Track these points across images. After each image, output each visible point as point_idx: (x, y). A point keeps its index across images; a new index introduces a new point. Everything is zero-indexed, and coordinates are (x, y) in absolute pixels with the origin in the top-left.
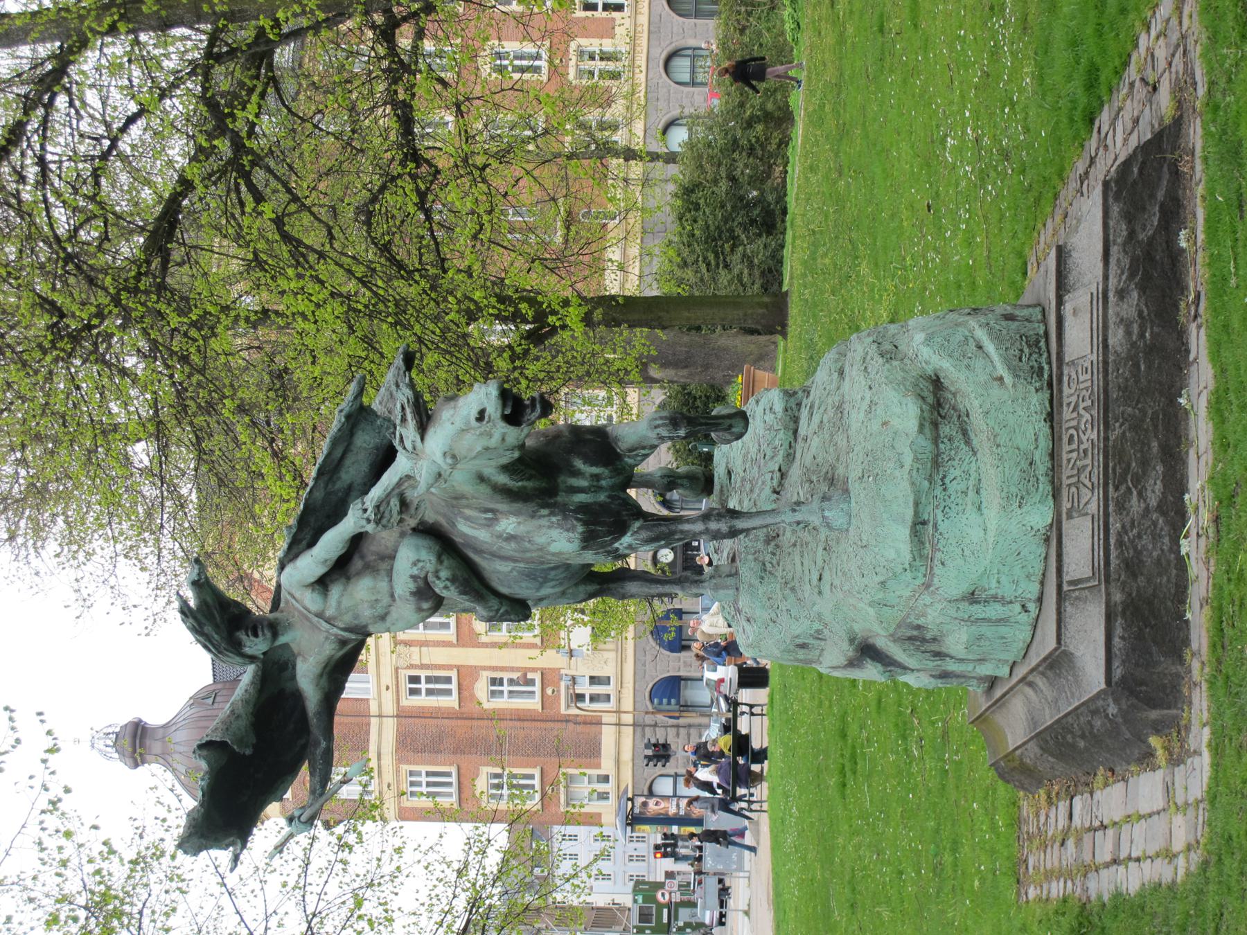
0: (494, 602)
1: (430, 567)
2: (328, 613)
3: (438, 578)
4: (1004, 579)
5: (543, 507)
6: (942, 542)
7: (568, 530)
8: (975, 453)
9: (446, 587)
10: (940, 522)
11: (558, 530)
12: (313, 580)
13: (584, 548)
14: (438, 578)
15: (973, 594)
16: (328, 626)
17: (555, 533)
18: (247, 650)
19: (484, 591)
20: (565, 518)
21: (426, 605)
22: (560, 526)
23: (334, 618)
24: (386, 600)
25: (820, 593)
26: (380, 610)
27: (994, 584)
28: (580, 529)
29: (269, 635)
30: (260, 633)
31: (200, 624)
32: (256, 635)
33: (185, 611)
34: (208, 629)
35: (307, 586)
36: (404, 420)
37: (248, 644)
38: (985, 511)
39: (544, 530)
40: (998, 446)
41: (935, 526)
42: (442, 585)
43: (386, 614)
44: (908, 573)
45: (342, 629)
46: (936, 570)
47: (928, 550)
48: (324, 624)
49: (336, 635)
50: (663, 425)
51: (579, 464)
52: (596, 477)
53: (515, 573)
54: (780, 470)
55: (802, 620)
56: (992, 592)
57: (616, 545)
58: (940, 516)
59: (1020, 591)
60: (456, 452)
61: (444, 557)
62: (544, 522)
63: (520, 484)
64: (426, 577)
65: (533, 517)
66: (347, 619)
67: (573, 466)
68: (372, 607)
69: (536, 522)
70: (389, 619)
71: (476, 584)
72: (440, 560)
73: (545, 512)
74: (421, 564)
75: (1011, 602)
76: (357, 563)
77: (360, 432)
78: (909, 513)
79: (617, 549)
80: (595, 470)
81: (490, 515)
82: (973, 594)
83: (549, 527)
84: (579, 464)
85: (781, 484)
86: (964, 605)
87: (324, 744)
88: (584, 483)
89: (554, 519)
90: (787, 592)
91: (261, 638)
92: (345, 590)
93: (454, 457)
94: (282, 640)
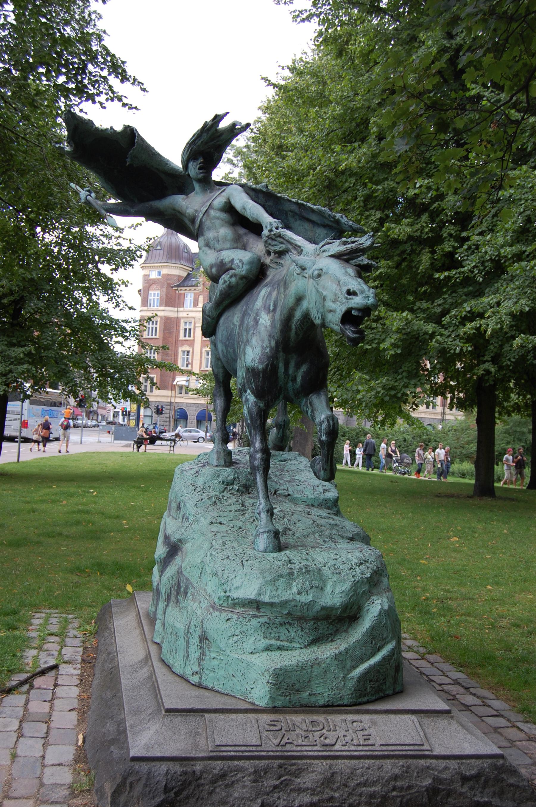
0: (215, 314)
5: (277, 343)
6: (244, 621)
7: (260, 359)
8: (306, 647)
9: (225, 282)
10: (258, 620)
11: (260, 352)
12: (233, 202)
13: (247, 369)
14: (231, 277)
15: (206, 639)
16: (204, 212)
17: (258, 350)
18: (191, 164)
19: (221, 308)
20: (269, 358)
21: (214, 270)
22: (263, 354)
23: (208, 216)
24: (218, 247)
25: (212, 523)
27: (213, 655)
28: (261, 367)
29: (200, 176)
30: (201, 171)
31: (209, 129)
32: (199, 169)
33: (218, 119)
34: (205, 136)
35: (229, 199)
36: (345, 243)
37: (195, 164)
38: (265, 654)
39: (260, 343)
40: (312, 666)
41: (255, 616)
42: (226, 279)
44: (223, 594)
46: (224, 614)
48: (205, 209)
49: (198, 216)
50: (329, 425)
51: (304, 368)
52: (294, 380)
53: (232, 326)
54: (289, 495)
55: (195, 508)
56: (207, 653)
57: (249, 391)
58: (262, 620)
59: (207, 672)
60: (322, 278)
61: (244, 280)
62: (266, 343)
63: (294, 327)
64: (231, 269)
65: (270, 336)
66: (207, 223)
67: (302, 364)
68: (214, 238)
69: (266, 338)
71: (226, 302)
73: (273, 343)
74: (241, 265)
75: (199, 665)
76: (242, 231)
77: (326, 232)
78: (266, 598)
79: (246, 392)
80: (299, 379)
81: (272, 308)
82: (206, 639)
83: (262, 347)
84: (304, 368)
85: (281, 495)
86: (198, 631)
88: (291, 371)
89: (268, 350)
90: (214, 500)
91: (198, 171)
92: (226, 222)
93: (319, 276)
94: (197, 186)
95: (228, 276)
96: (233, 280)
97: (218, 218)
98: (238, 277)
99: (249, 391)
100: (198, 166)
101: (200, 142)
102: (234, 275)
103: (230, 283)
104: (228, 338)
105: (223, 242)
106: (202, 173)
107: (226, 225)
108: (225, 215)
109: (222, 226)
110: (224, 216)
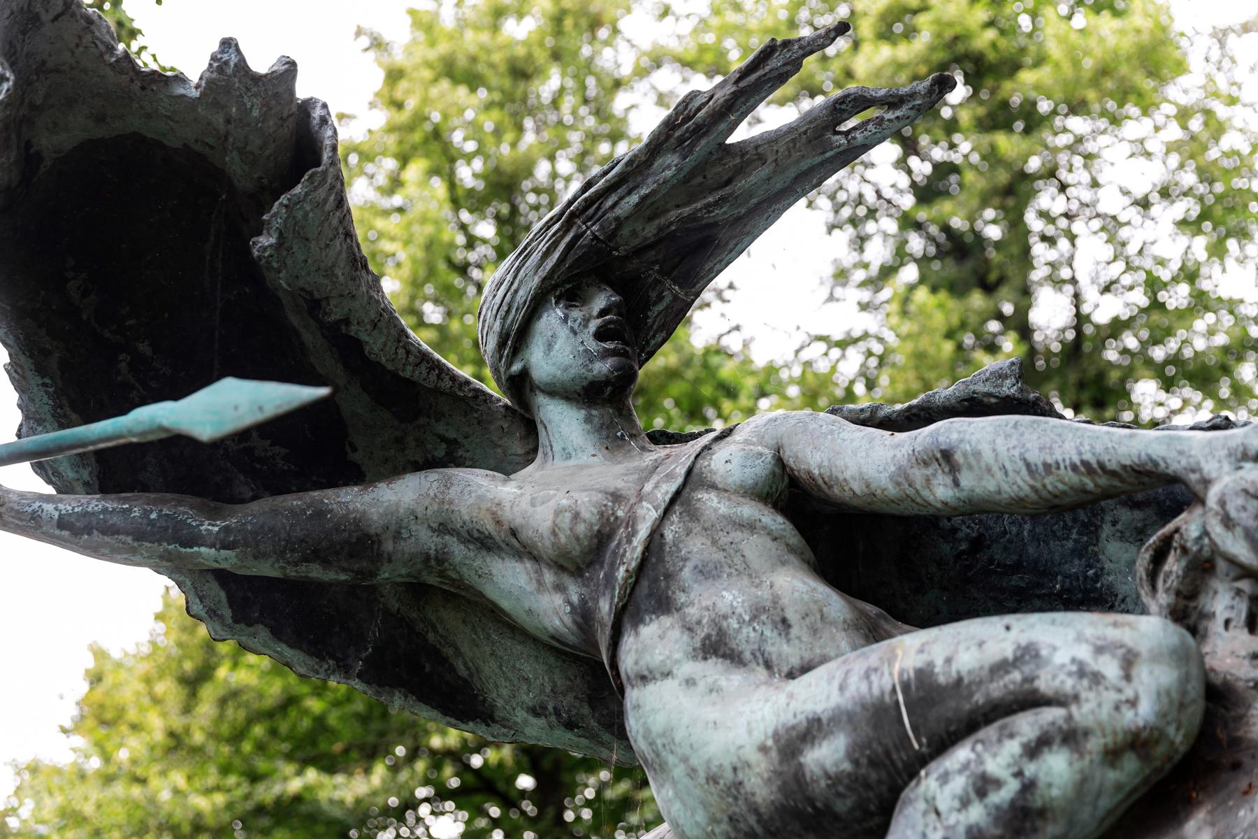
1: (1092, 709)
2: (711, 503)
3: (1034, 750)
9: (983, 785)
14: (1034, 750)
23: (693, 514)
24: (788, 652)
26: (746, 638)
29: (602, 368)
30: (609, 345)
31: (700, 131)
32: (600, 335)
34: (669, 165)
37: (576, 314)
43: (734, 658)
45: (656, 533)
49: (631, 522)
61: (1131, 764)
64: (1030, 700)
70: (712, 670)
72: (1138, 742)
74: (1110, 668)
87: (210, 527)
91: (593, 345)
92: (791, 549)
94: (564, 423)
95: (1013, 747)
96: (1057, 768)
97: (751, 527)
98: (1094, 745)
100: (594, 325)
101: (634, 199)
102: (1071, 737)
103: (1029, 786)
105: (814, 631)
106: (613, 353)
107: (792, 558)
108: (780, 519)
109: (783, 563)
110: (773, 520)
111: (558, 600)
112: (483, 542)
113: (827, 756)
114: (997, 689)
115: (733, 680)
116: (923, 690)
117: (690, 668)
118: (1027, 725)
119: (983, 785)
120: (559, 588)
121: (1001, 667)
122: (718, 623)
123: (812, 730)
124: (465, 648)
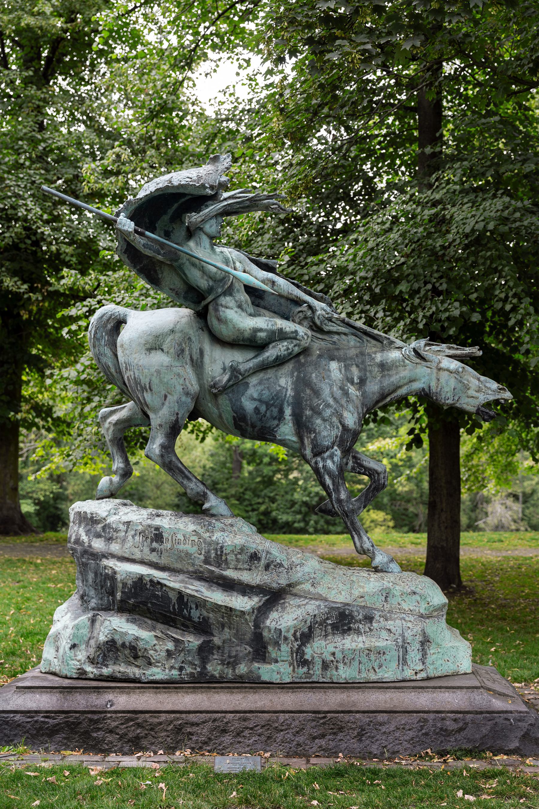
3: (295, 346)
4: (434, 656)
9: (288, 349)
14: (295, 346)
17: (356, 415)
27: (432, 652)
42: (290, 347)
43: (242, 309)
44: (426, 605)
47: (435, 614)
53: (278, 388)
62: (360, 410)
64: (295, 339)
65: (363, 404)
70: (239, 310)
74: (306, 337)
79: (333, 448)
81: (356, 380)
86: (419, 638)
99: (336, 448)
104: (273, 398)
111: (206, 282)
112: (194, 265)
113: (262, 335)
114: (292, 335)
115: (243, 314)
116: (281, 330)
117: (236, 309)
118: (295, 342)
119: (288, 349)
120: (207, 281)
121: (292, 332)
122: (241, 302)
123: (261, 330)
124: (165, 274)
